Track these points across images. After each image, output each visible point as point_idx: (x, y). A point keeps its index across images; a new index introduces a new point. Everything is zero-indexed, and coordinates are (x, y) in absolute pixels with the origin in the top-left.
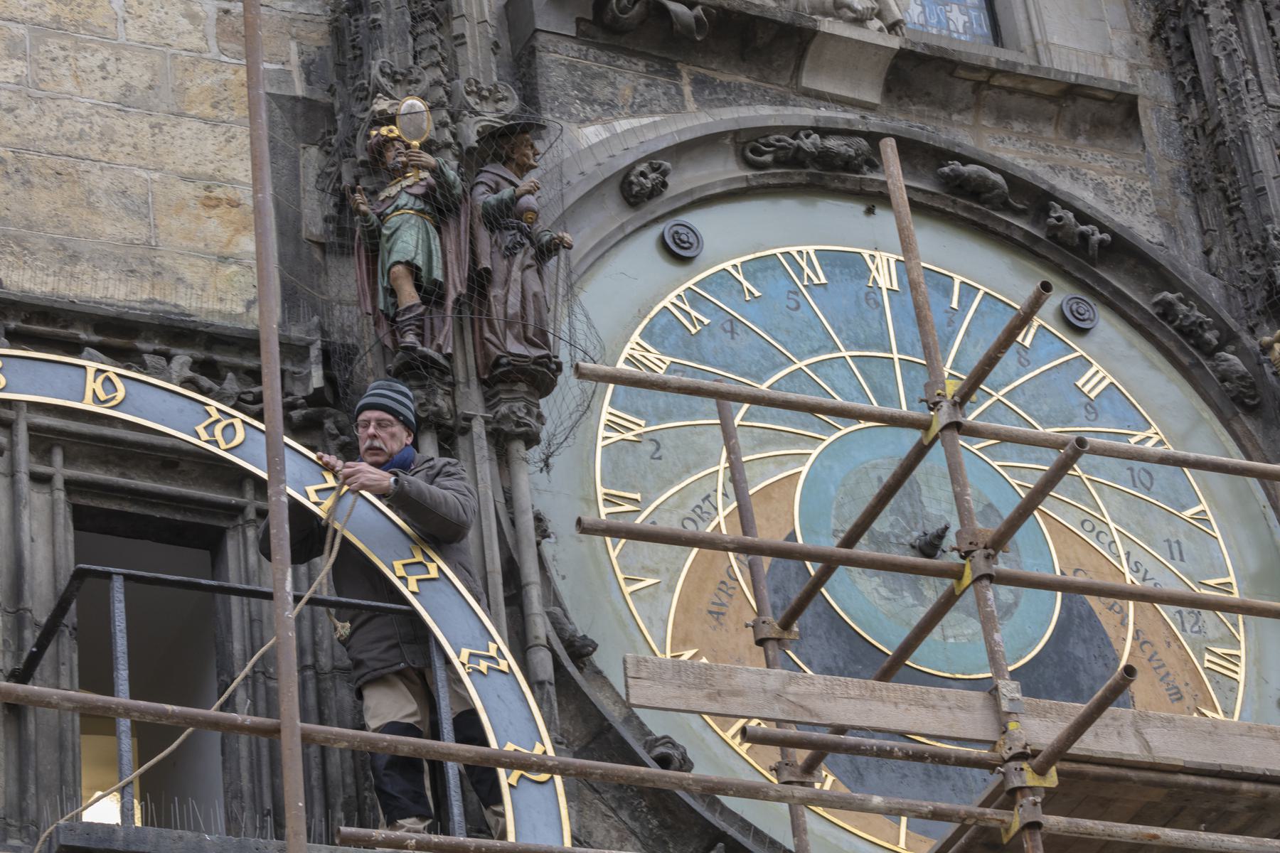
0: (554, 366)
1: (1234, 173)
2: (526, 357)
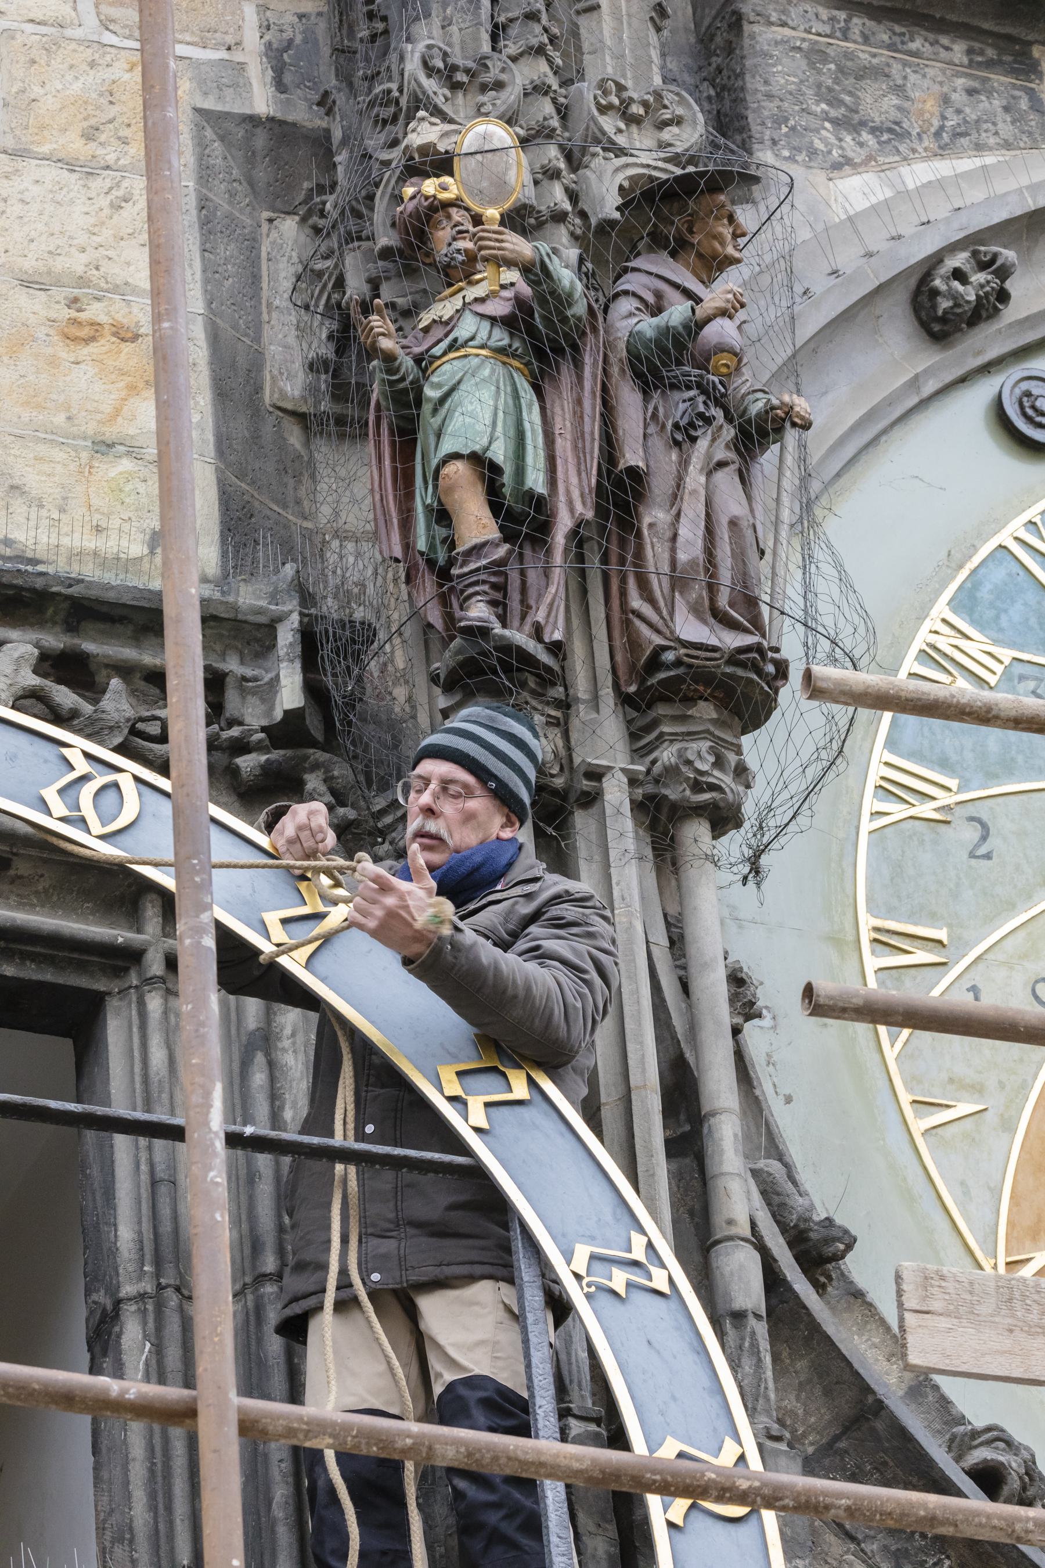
0: (770, 668)
2: (714, 649)
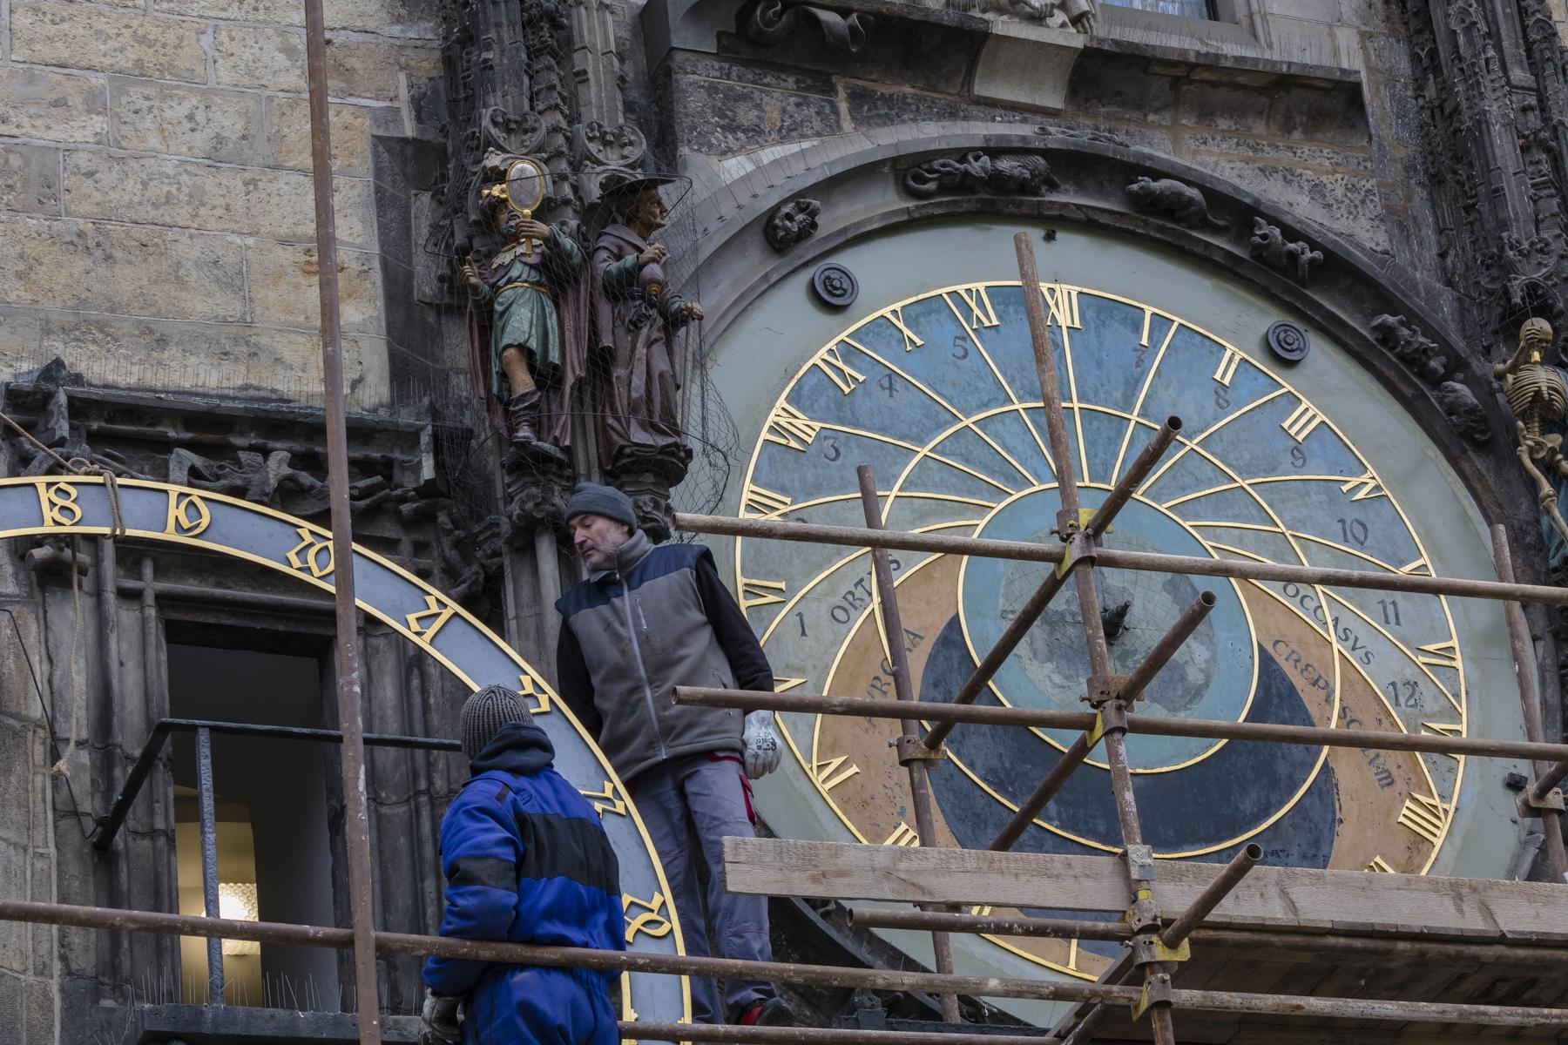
1: (1471, 165)
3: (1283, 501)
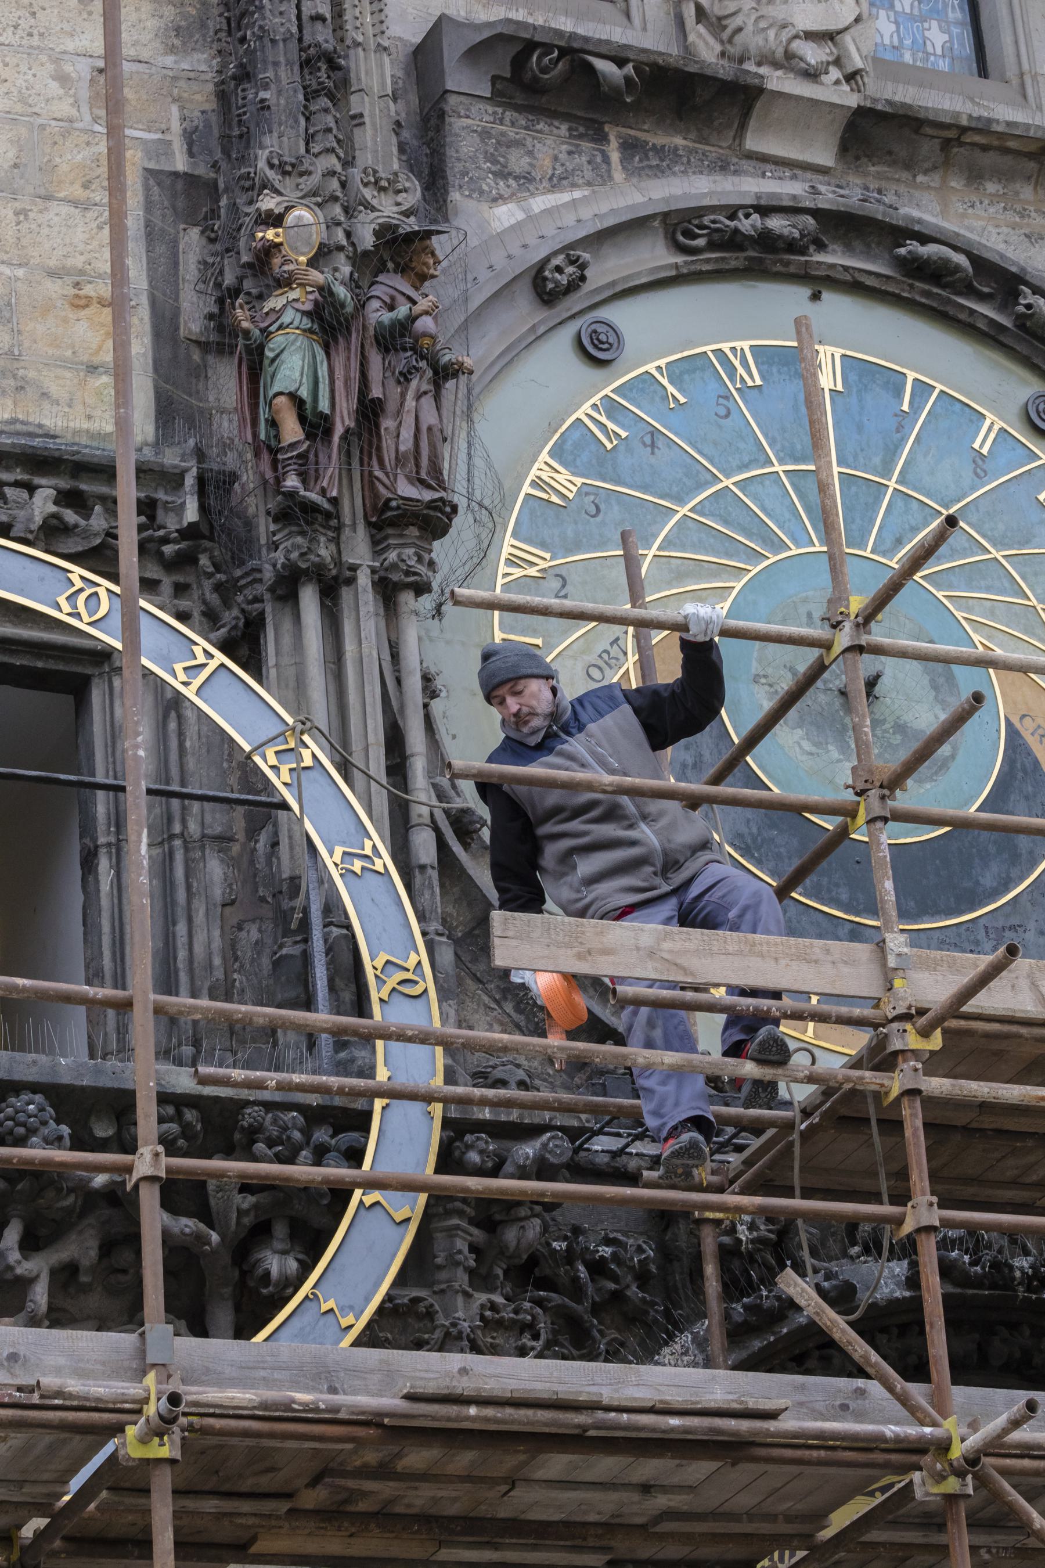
0: (448, 509)
2: (418, 501)
3: (1036, 574)
